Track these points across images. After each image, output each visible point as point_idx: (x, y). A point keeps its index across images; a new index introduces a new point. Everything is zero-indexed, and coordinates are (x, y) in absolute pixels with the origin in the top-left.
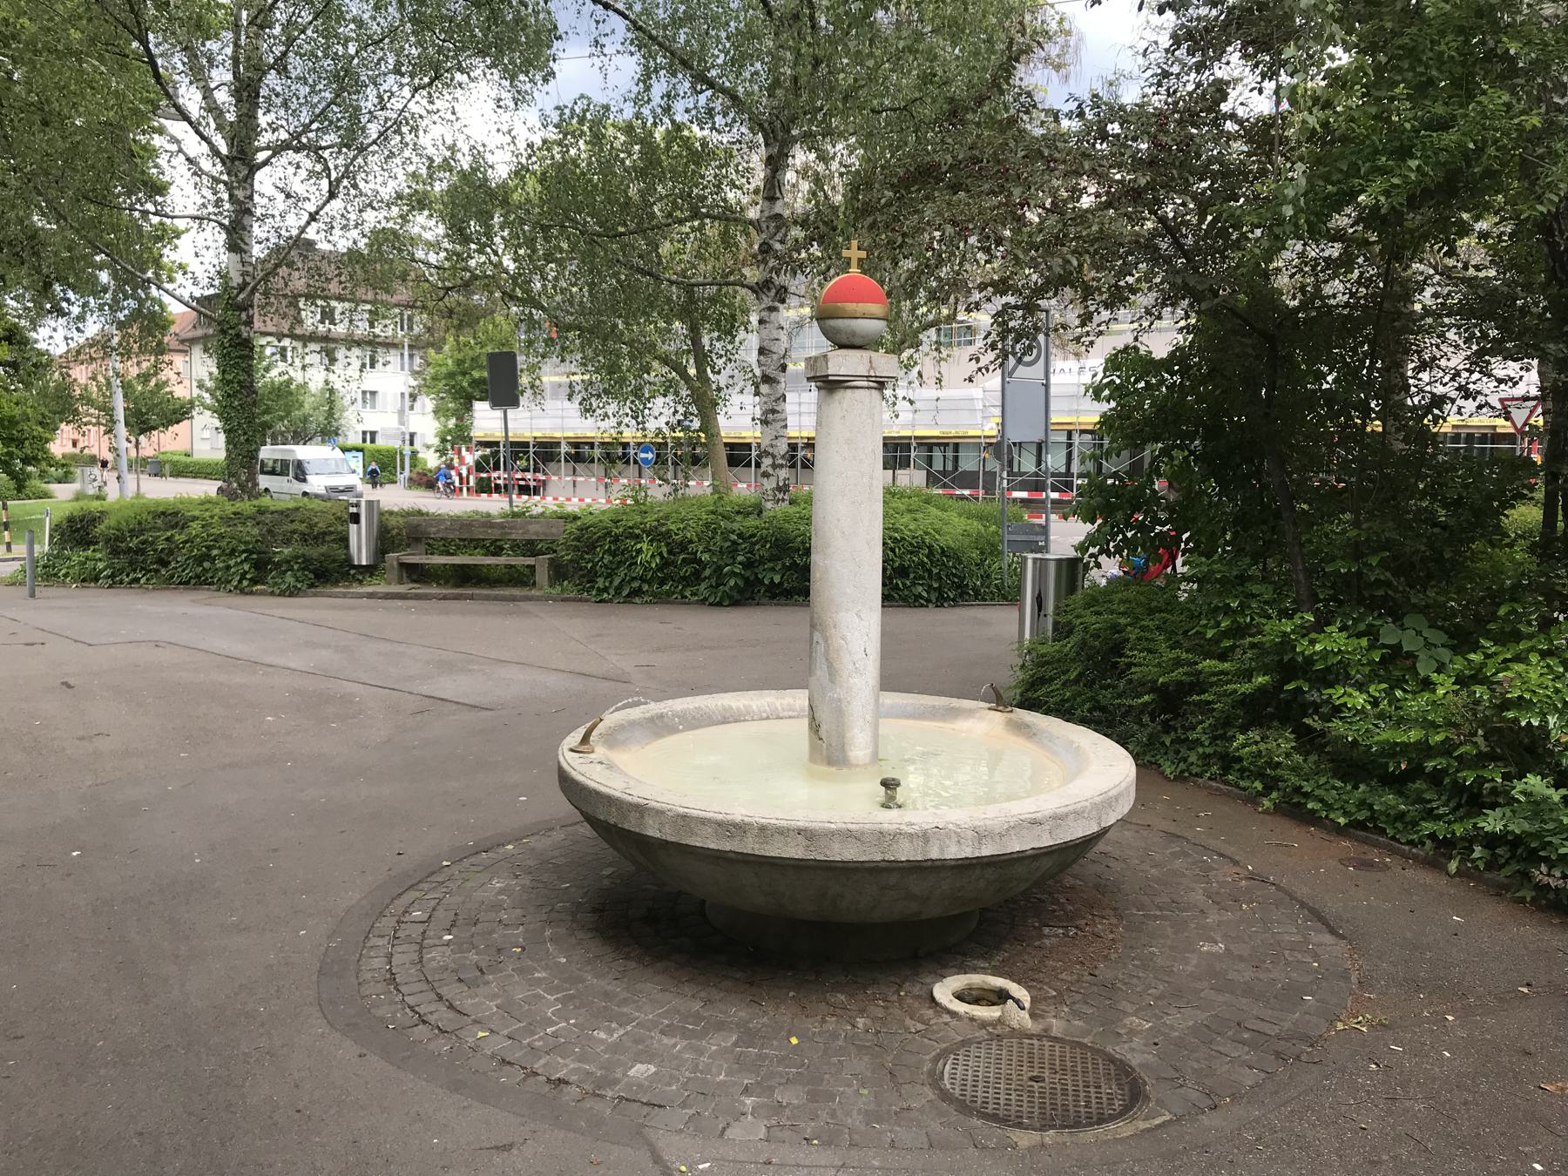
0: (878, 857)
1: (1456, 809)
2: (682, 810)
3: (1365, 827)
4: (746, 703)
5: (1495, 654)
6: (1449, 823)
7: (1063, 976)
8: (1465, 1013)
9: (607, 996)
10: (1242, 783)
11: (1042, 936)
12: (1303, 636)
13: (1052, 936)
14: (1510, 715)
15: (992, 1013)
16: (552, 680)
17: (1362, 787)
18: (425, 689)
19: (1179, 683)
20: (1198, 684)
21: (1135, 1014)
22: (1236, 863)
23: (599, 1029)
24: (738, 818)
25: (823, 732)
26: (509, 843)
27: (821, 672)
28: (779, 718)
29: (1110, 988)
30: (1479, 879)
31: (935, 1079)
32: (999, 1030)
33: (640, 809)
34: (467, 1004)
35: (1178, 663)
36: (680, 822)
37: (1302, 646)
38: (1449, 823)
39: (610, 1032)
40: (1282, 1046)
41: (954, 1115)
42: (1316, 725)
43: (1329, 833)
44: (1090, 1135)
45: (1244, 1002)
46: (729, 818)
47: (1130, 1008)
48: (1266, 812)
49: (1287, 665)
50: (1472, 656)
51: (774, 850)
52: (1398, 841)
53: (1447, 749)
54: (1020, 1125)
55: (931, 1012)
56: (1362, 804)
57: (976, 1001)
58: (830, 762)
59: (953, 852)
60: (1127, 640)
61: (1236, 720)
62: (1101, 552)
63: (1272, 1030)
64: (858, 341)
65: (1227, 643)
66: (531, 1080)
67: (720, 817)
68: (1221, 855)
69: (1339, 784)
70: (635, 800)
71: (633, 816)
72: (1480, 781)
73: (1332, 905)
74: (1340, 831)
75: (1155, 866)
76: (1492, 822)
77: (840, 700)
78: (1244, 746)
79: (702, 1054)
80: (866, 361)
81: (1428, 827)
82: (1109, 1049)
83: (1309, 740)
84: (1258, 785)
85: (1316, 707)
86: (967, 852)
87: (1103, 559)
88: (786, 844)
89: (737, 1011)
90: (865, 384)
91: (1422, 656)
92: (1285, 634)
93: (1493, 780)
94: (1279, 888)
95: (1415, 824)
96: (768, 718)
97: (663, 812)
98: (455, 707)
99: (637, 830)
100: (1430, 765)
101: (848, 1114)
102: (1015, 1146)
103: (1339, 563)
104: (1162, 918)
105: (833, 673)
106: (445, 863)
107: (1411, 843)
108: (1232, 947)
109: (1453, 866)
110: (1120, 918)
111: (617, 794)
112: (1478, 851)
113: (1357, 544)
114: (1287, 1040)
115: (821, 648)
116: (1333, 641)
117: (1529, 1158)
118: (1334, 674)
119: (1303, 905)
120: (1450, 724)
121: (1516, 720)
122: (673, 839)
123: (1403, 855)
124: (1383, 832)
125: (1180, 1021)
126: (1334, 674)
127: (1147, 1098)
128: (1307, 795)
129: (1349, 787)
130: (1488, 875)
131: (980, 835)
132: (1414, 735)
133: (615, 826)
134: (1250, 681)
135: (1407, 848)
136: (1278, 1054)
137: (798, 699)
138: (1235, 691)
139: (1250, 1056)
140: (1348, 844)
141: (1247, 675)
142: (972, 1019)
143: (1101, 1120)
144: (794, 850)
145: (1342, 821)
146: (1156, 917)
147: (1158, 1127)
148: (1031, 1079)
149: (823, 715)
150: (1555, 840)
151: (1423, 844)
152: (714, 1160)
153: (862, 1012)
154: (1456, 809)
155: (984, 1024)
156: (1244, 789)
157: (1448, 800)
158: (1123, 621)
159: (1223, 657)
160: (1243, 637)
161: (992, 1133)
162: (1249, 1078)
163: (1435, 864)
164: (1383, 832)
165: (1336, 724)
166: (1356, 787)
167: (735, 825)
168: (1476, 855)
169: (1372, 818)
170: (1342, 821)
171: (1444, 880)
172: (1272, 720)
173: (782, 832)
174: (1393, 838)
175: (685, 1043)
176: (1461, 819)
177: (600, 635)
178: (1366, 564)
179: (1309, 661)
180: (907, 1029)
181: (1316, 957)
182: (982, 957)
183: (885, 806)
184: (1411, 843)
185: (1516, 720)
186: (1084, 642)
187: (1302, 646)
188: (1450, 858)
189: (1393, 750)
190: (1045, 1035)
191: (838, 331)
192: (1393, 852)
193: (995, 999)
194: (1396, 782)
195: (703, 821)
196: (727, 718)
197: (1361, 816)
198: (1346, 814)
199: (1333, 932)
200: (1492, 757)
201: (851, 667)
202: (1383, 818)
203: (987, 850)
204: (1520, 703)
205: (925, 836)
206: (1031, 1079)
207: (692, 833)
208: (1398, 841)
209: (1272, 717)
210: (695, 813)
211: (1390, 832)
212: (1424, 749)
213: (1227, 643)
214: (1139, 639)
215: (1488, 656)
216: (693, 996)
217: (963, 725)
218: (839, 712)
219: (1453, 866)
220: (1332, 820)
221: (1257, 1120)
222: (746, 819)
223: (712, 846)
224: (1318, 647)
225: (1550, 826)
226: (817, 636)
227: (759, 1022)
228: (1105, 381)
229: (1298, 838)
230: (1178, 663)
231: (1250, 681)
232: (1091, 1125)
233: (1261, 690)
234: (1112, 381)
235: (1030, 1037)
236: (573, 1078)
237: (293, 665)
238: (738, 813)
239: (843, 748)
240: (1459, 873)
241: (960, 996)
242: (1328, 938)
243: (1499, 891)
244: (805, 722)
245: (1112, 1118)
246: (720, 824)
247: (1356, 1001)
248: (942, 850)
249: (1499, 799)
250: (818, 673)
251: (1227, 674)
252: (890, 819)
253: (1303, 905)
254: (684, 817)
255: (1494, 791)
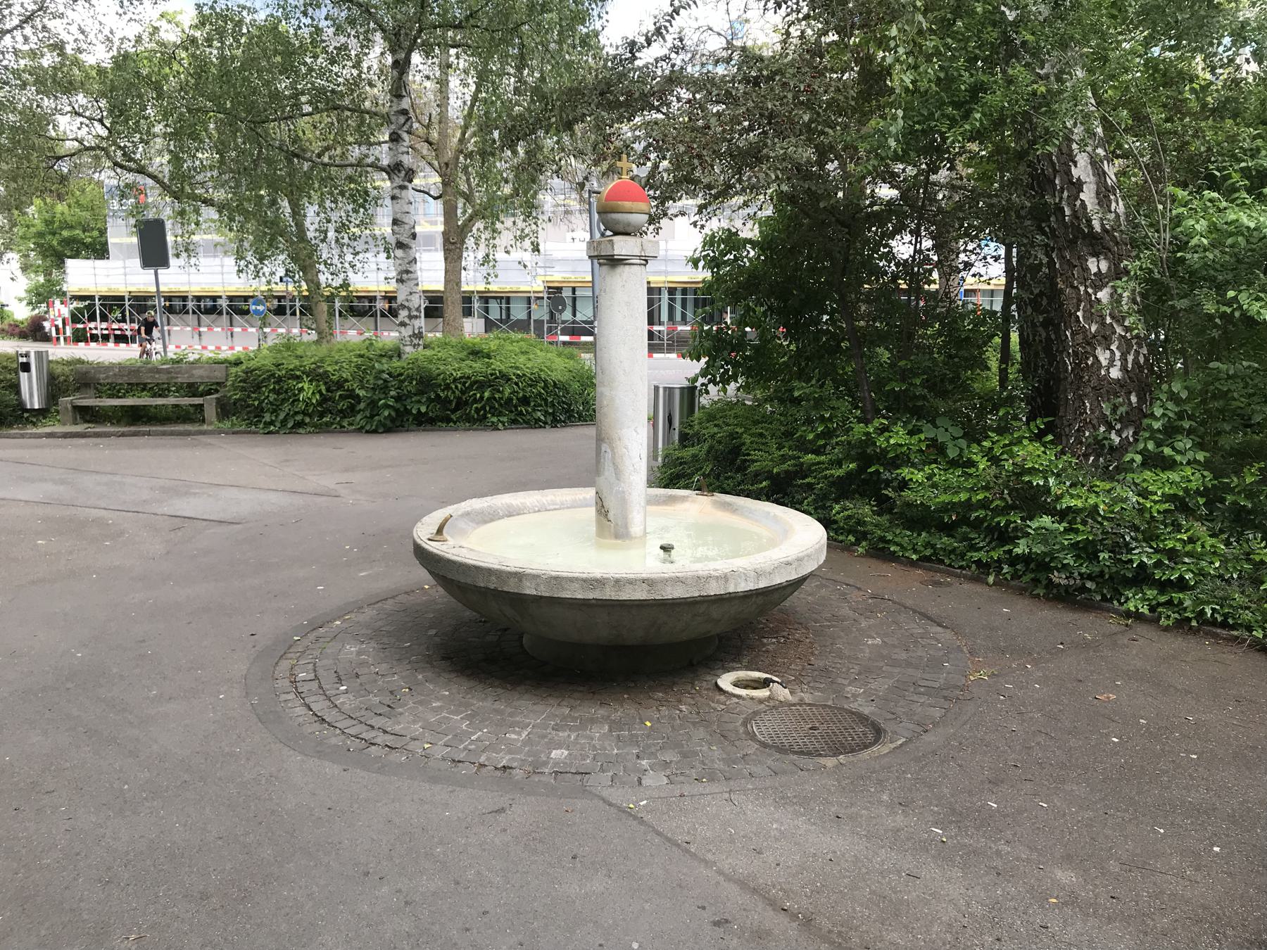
0: (696, 594)
1: (990, 542)
2: (554, 574)
3: (930, 560)
4: (523, 501)
5: (998, 441)
6: (988, 552)
7: (793, 667)
8: (1035, 662)
9: (497, 711)
10: (841, 538)
11: (764, 645)
12: (879, 435)
13: (771, 643)
14: (1027, 479)
15: (763, 693)
16: (273, 497)
17: (924, 534)
18: (166, 510)
19: (786, 472)
20: (802, 471)
21: (849, 685)
22: (859, 589)
23: (509, 732)
24: (599, 576)
25: (611, 516)
26: (335, 620)
27: (608, 472)
28: (546, 510)
29: (825, 671)
30: (1008, 587)
31: (752, 737)
32: (772, 704)
33: (519, 576)
34: (397, 728)
35: (784, 458)
36: (554, 582)
37: (881, 441)
38: (988, 552)
39: (519, 734)
40: (945, 693)
41: (778, 756)
42: (890, 495)
43: (905, 566)
44: (865, 754)
45: (910, 671)
46: (591, 575)
47: (846, 682)
48: (861, 556)
49: (865, 454)
50: (985, 443)
51: (625, 595)
52: (954, 567)
53: (984, 504)
54: (820, 755)
55: (722, 697)
56: (928, 545)
57: (746, 687)
58: (617, 536)
59: (743, 587)
60: (744, 444)
61: (830, 495)
62: (710, 381)
63: (937, 685)
64: (629, 230)
65: (821, 442)
66: (484, 770)
67: (585, 576)
68: (847, 585)
69: (909, 533)
70: (513, 570)
71: (512, 581)
72: (1008, 523)
73: (933, 611)
74: (913, 564)
75: (810, 595)
76: (1021, 548)
77: (623, 492)
78: (838, 513)
79: (592, 739)
80: (639, 245)
81: (976, 556)
82: (846, 707)
83: (884, 506)
84: (852, 538)
85: (888, 483)
86: (751, 586)
87: (711, 387)
88: (634, 590)
89: (595, 710)
90: (638, 261)
91: (950, 445)
92: (868, 434)
93: (1015, 522)
94: (894, 602)
95: (962, 556)
96: (539, 511)
97: (538, 576)
98: (205, 523)
99: (516, 591)
100: (974, 515)
101: (713, 761)
102: (825, 767)
103: (894, 384)
104: (833, 626)
105: (618, 473)
106: (296, 638)
107: (961, 567)
108: (885, 640)
109: (991, 579)
110: (807, 628)
111: (496, 567)
112: (1006, 569)
113: (904, 370)
114: (947, 689)
115: (609, 455)
116: (899, 437)
117: (1107, 735)
118: (901, 459)
119: (915, 611)
120: (987, 488)
121: (1030, 482)
122: (547, 595)
123: (958, 576)
124: (942, 562)
125: (881, 685)
126: (901, 459)
127: (885, 730)
128: (889, 542)
129: (915, 535)
130: (1013, 583)
131: (759, 574)
132: (963, 496)
133: (495, 590)
134: (841, 467)
135: (959, 571)
136: (945, 698)
137: (590, 493)
138: (832, 475)
139: (931, 701)
140: (920, 572)
141: (839, 464)
142: (752, 698)
143: (866, 747)
144: (640, 594)
145: (914, 557)
146: (829, 627)
147: (901, 745)
148: (811, 729)
149: (611, 503)
150: (1061, 555)
151: (970, 567)
152: (647, 799)
153: (680, 701)
154: (990, 542)
155: (761, 701)
156: (841, 542)
157: (985, 537)
158: (740, 430)
159: (817, 452)
160: (831, 438)
161: (803, 761)
162: (937, 713)
163: (978, 580)
164: (942, 562)
165: (906, 493)
166: (919, 535)
167: (597, 580)
168: (1004, 571)
169: (935, 554)
170: (914, 557)
171: (987, 589)
172: (854, 494)
173: (631, 582)
174: (950, 565)
175: (575, 734)
176: (993, 549)
177: (287, 461)
178: (911, 384)
179: (884, 451)
180: (715, 709)
181: (938, 641)
182: (733, 661)
183: (664, 561)
184: (961, 567)
185: (1030, 482)
186: (711, 447)
187: (881, 441)
188: (988, 574)
189: (947, 508)
190: (801, 703)
191: (617, 222)
192: (950, 574)
193: (756, 685)
194: (949, 529)
195: (572, 580)
196: (511, 513)
197: (928, 552)
198: (915, 551)
199: (939, 625)
200: (1013, 507)
201: (631, 468)
202: (941, 553)
203: (762, 584)
204: (1032, 471)
205: (725, 578)
206: (811, 729)
207: (564, 589)
208: (954, 567)
209: (854, 492)
210: (565, 574)
211: (947, 561)
212: (968, 505)
213: (821, 442)
214: (751, 443)
215: (993, 443)
216: (559, 705)
217: (680, 507)
218: (623, 502)
219: (991, 579)
220: (908, 558)
221: (954, 734)
222: (605, 576)
223: (579, 596)
224: (892, 441)
225: (1057, 547)
226: (604, 447)
227: (618, 714)
228: (703, 254)
229: (890, 572)
230: (784, 458)
231: (841, 467)
232: (860, 750)
233: (849, 474)
234: (708, 255)
235: (794, 705)
236: (515, 765)
237: (20, 497)
238: (597, 573)
239: (626, 526)
240: (995, 584)
241: (736, 684)
242: (939, 629)
243: (1021, 591)
244: (592, 512)
245: (871, 745)
246: (585, 580)
247: (972, 663)
248: (736, 586)
249: (1022, 533)
250: (607, 473)
251: (823, 463)
252: (669, 570)
253: (915, 611)
254: (556, 578)
255: (1016, 529)
